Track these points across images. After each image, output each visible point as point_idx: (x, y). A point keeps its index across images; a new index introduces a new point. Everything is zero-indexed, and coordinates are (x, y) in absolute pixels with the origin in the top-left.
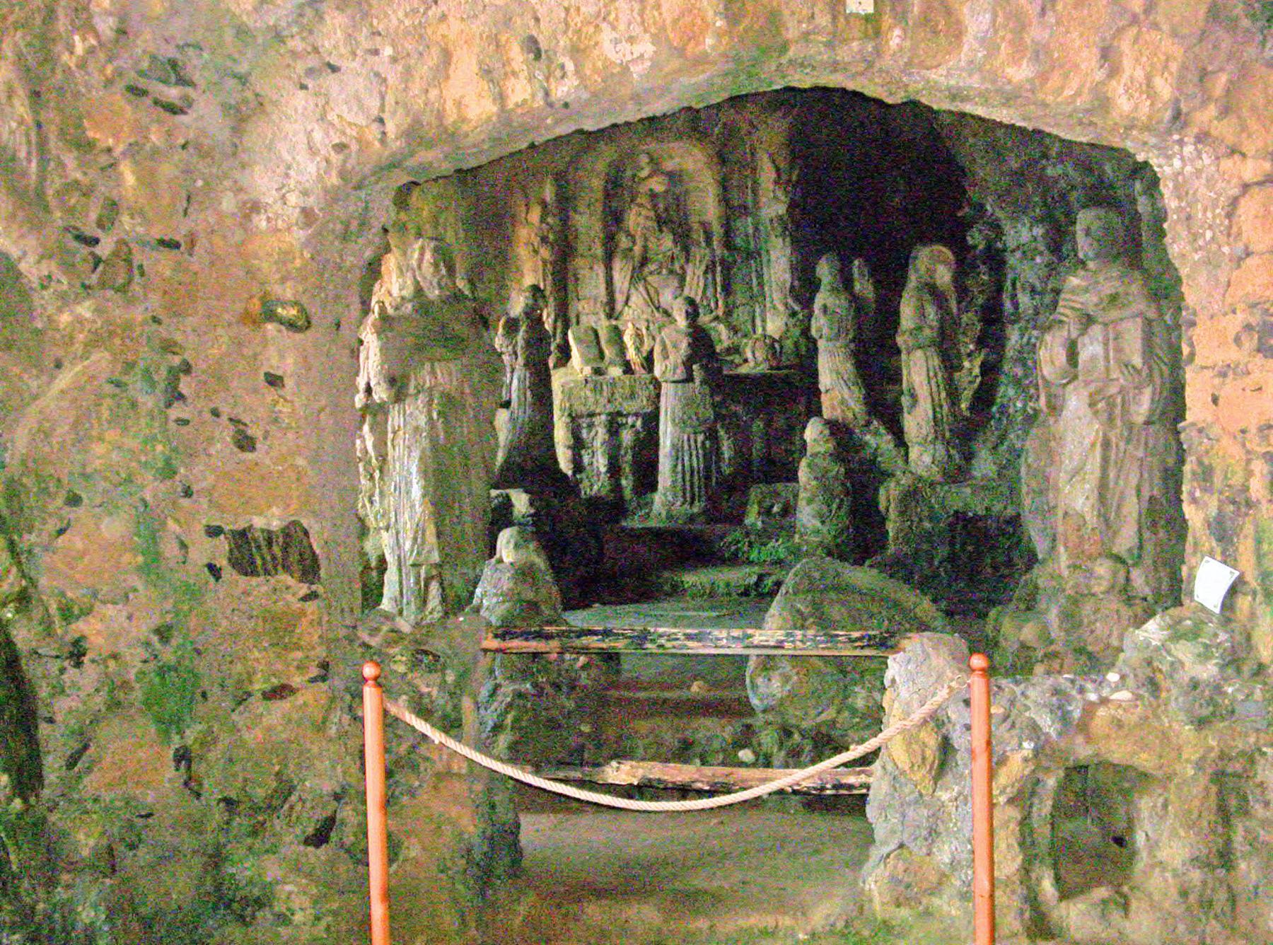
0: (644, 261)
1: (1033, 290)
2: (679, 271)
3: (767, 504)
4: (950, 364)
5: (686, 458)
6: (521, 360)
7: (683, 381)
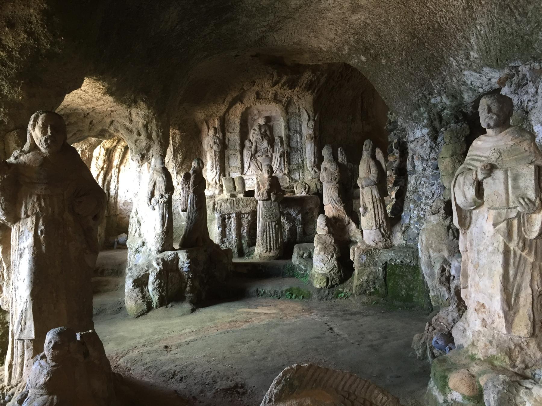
0: (256, 151)
1: (423, 159)
2: (270, 156)
3: (301, 253)
4: (383, 193)
5: (268, 233)
6: (191, 191)
7: (267, 200)
